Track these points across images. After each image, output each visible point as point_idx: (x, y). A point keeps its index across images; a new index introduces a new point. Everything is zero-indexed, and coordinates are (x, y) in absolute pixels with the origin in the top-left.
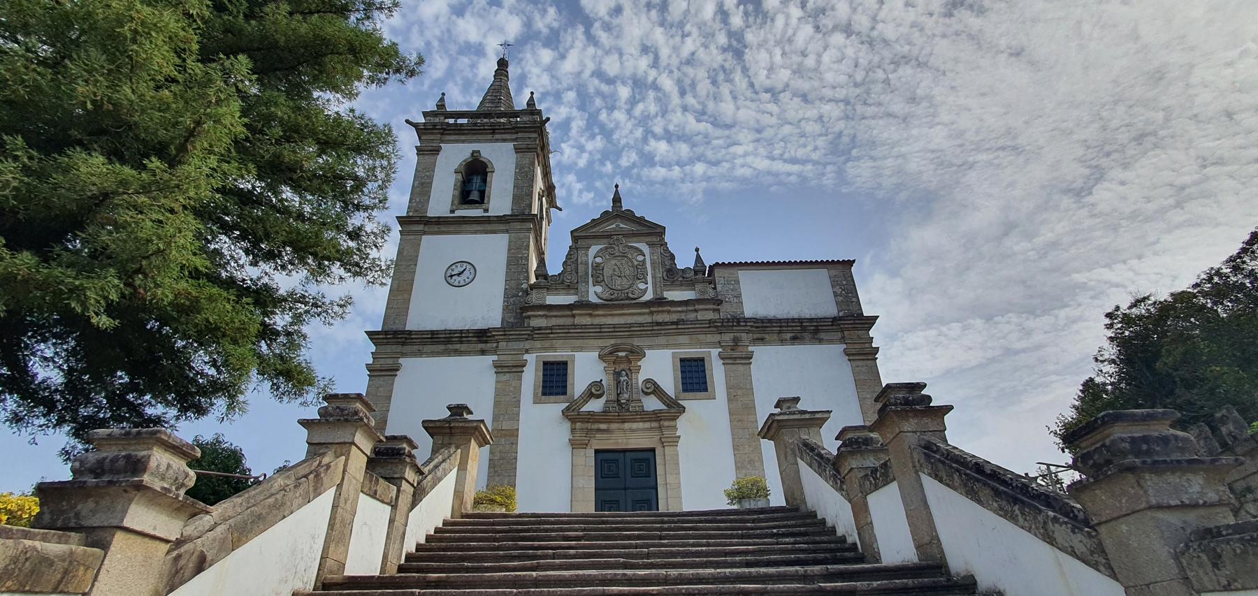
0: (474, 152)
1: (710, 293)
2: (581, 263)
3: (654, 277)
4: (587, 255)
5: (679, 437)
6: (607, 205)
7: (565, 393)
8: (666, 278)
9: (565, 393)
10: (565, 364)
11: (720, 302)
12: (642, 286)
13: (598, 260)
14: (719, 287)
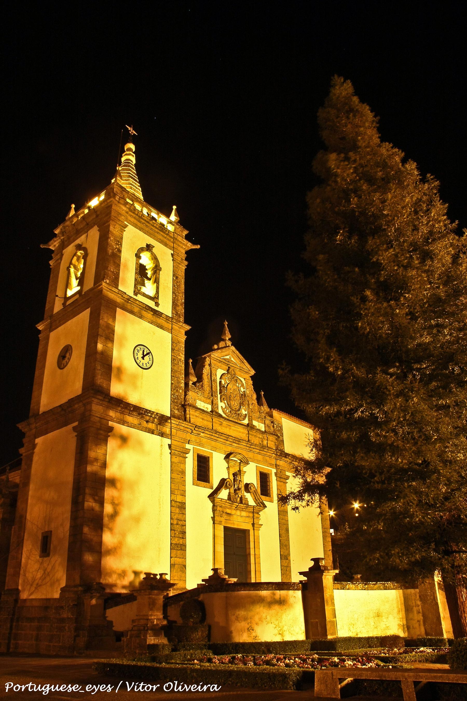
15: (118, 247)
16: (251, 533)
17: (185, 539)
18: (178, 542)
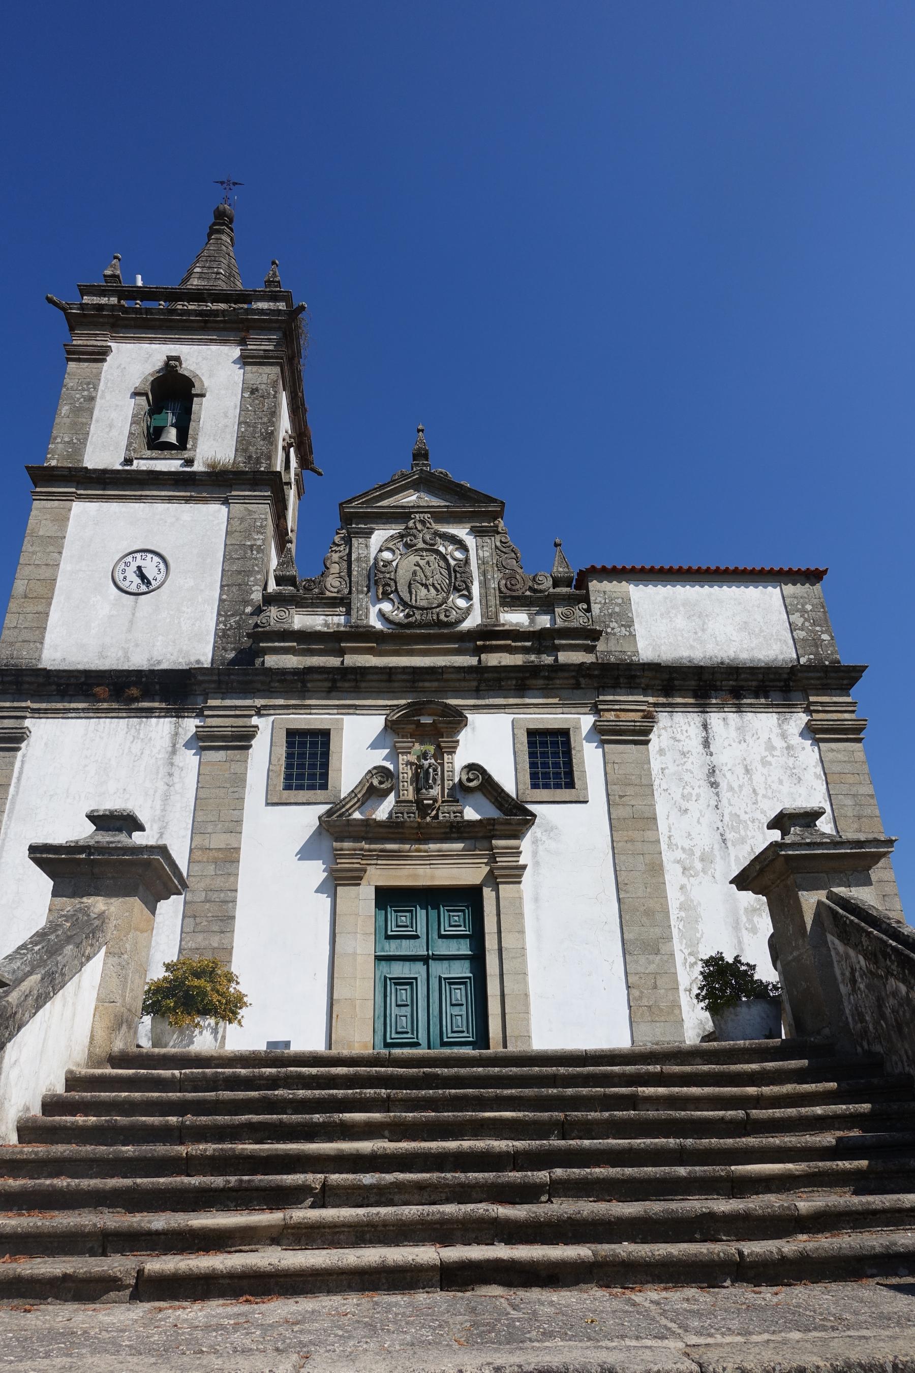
0: (170, 358)
1: (578, 619)
2: (358, 559)
3: (484, 584)
4: (367, 546)
5: (524, 867)
6: (404, 464)
7: (324, 786)
8: (503, 589)
9: (324, 786)
10: (325, 734)
11: (595, 635)
12: (462, 603)
13: (387, 555)
14: (596, 609)
15: (86, 393)
16: (488, 894)
17: (228, 935)
18: (204, 944)
